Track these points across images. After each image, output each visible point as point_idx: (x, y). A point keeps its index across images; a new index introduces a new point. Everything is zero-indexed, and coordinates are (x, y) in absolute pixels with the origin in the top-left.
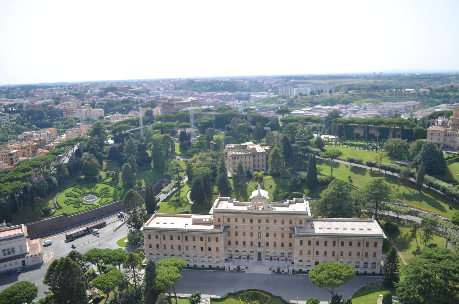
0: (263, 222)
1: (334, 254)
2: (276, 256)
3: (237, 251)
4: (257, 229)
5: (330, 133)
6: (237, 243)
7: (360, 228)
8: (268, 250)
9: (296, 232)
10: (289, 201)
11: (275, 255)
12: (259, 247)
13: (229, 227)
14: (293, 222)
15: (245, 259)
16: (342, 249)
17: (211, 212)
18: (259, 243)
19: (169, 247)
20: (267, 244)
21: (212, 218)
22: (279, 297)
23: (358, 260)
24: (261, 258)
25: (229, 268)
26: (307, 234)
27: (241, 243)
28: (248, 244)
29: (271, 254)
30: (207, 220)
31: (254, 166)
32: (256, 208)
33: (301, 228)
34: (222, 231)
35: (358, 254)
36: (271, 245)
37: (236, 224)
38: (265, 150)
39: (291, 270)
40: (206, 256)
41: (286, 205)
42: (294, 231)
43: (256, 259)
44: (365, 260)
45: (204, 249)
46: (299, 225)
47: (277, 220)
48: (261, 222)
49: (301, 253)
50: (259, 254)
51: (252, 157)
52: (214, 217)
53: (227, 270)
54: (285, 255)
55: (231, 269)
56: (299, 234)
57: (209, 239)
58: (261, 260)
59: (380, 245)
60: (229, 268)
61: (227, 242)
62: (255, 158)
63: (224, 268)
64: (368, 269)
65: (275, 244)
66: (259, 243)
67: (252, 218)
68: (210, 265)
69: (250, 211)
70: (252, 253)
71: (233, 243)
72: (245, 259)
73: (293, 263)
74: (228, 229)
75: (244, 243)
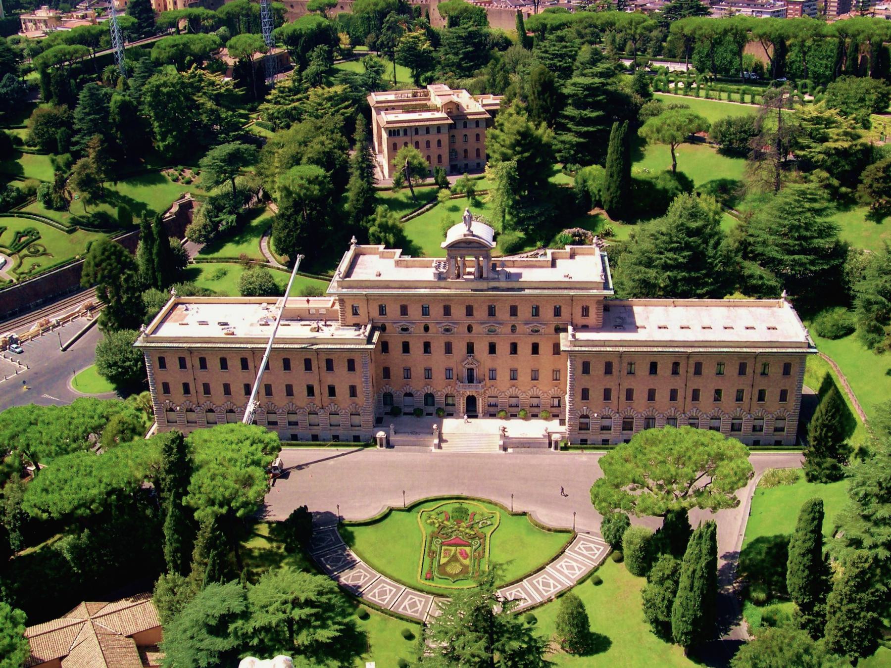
5: (672, 57)
7: (749, 325)
10: (553, 254)
14: (565, 312)
16: (696, 383)
17: (333, 287)
18: (471, 371)
19: (217, 390)
21: (337, 307)
22: (524, 514)
24: (475, 411)
30: (323, 311)
31: (453, 152)
38: (484, 106)
44: (757, 411)
46: (581, 321)
47: (519, 308)
49: (585, 395)
51: (444, 131)
52: (342, 301)
62: (454, 132)
64: (763, 433)
67: (447, 303)
71: (397, 372)
72: (431, 414)
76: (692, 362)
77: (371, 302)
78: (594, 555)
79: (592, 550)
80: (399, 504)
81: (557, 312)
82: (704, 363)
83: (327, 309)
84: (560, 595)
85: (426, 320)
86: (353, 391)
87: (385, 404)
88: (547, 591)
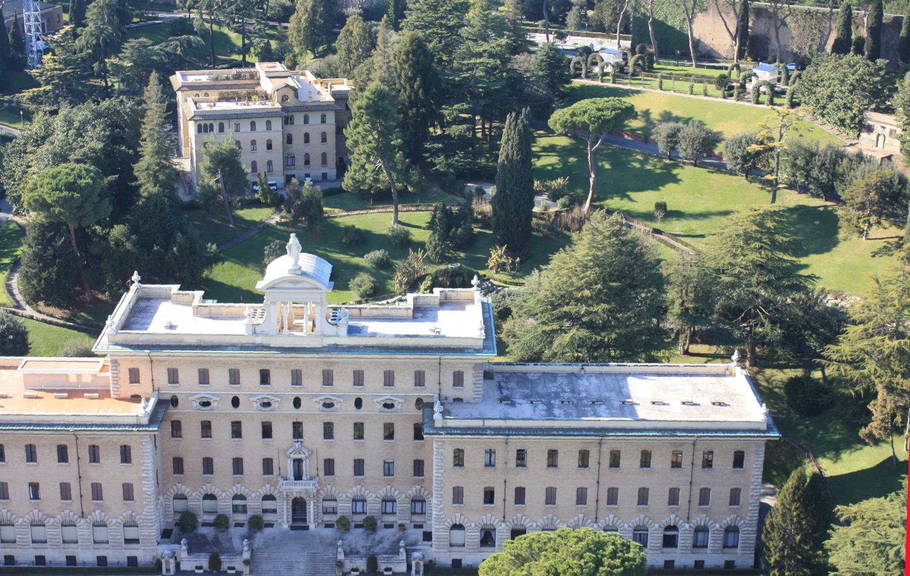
0: (312, 383)
1: (581, 497)
2: (364, 513)
3: (210, 497)
6: (208, 465)
8: (329, 490)
9: (437, 416)
10: (415, 299)
11: (359, 509)
12: (298, 476)
13: (174, 401)
14: (431, 378)
15: (241, 525)
16: (612, 478)
18: (298, 462)
20: (329, 466)
23: (672, 519)
24: (305, 520)
25: (178, 565)
26: (478, 423)
27: (223, 465)
28: (253, 467)
29: (344, 507)
30: (87, 379)
33: (458, 400)
35: (673, 497)
36: (344, 468)
37: (203, 392)
39: (417, 564)
40: (83, 521)
41: (404, 313)
42: (433, 413)
43: (286, 526)
44: (699, 519)
45: (75, 492)
46: (451, 392)
48: (304, 381)
49: (458, 496)
50: (299, 506)
52: (115, 362)
53: (168, 570)
54: (398, 507)
55: (185, 566)
56: (452, 423)
57: (94, 455)
58: (307, 528)
59: (755, 463)
60: (178, 565)
61: (170, 464)
63: (159, 563)
64: (708, 550)
65: (359, 467)
66: (298, 462)
68: (102, 553)
69: (258, 340)
70: (269, 505)
71: (193, 465)
72: (241, 525)
73: (428, 536)
74: (172, 410)
75: (238, 465)
76: (606, 450)
77: (155, 364)
81: (419, 379)
82: (622, 451)
83: (94, 376)
85: (234, 391)
86: (128, 492)
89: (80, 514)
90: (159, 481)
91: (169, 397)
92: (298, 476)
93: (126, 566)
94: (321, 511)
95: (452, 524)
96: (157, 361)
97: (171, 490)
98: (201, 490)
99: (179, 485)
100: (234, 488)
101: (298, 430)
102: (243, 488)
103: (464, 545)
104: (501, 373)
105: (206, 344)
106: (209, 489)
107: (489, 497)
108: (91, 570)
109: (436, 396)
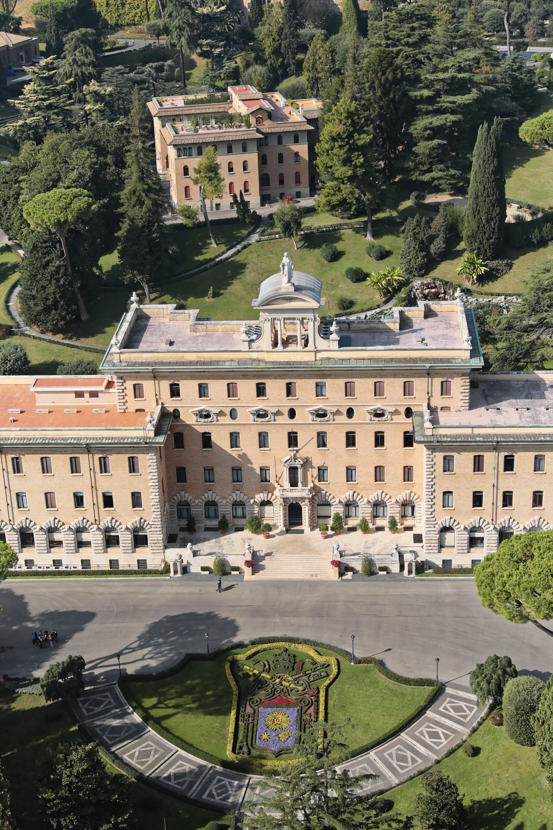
3: (211, 504)
4: (285, 419)
10: (401, 313)
18: (293, 470)
24: (301, 524)
32: (275, 344)
34: (152, 434)
37: (203, 405)
39: (410, 565)
45: (87, 501)
56: (442, 431)
61: (174, 473)
65: (350, 473)
69: (254, 356)
78: (465, 717)
79: (462, 710)
80: (202, 650)
81: (407, 390)
84: (421, 773)
87: (180, 517)
88: (402, 767)
89: (93, 521)
90: (165, 490)
91: (171, 410)
92: (294, 483)
93: (136, 568)
94: (316, 515)
95: (441, 526)
96: (159, 376)
97: (175, 498)
98: (203, 497)
99: (183, 493)
100: (234, 495)
101: (293, 440)
102: (242, 495)
103: (454, 547)
104: (486, 382)
105: (206, 360)
106: (210, 496)
107: (478, 500)
108: (103, 573)
109: (425, 405)
